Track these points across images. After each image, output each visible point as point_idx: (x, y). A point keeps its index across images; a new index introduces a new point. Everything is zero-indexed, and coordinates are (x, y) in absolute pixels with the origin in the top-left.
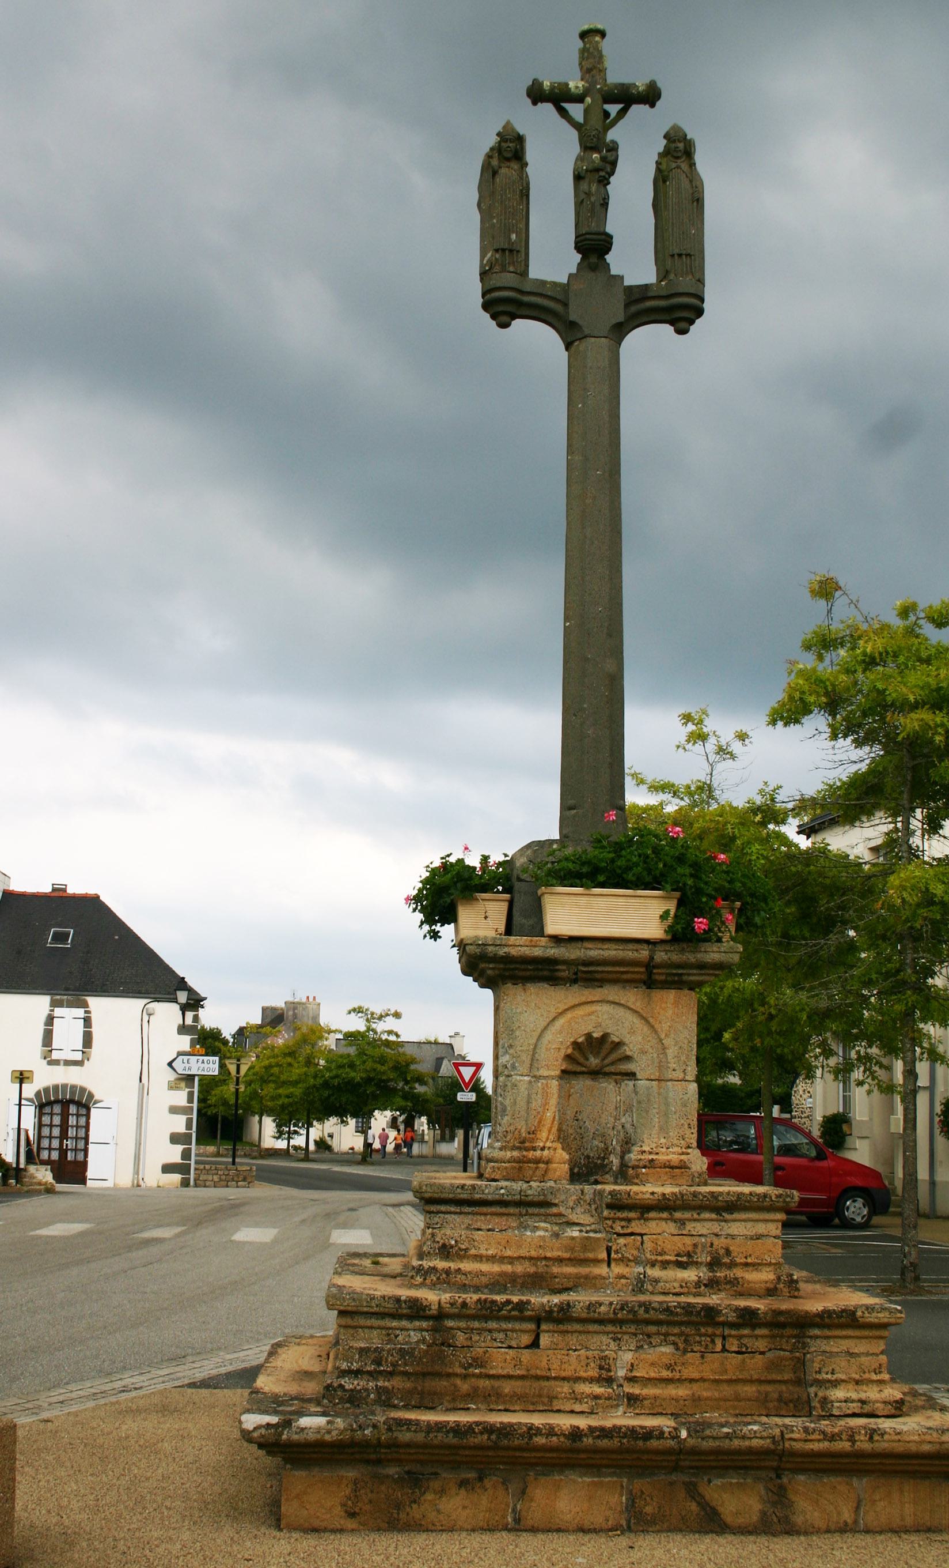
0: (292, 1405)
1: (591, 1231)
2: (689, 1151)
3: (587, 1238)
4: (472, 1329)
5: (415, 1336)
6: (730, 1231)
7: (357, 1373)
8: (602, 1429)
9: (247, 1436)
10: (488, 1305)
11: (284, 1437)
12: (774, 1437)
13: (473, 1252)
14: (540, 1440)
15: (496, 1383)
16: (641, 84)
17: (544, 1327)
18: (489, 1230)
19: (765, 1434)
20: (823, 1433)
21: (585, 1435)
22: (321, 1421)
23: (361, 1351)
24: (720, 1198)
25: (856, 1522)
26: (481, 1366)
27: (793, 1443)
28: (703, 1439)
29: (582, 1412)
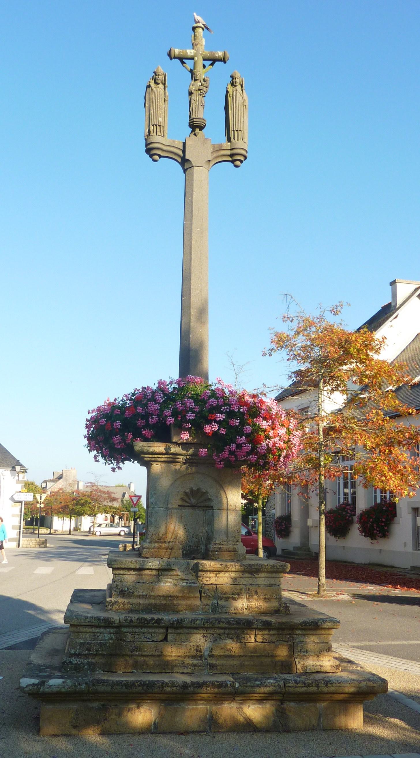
0: (46, 672)
1: (192, 583)
2: (238, 543)
3: (190, 586)
4: (135, 632)
5: (107, 636)
6: (258, 583)
7: (78, 655)
8: (198, 683)
9: (22, 689)
10: (143, 621)
11: (41, 690)
12: (280, 686)
13: (136, 593)
14: (168, 689)
15: (146, 659)
16: (220, 54)
17: (169, 631)
18: (144, 583)
19: (276, 684)
20: (304, 683)
21: (190, 686)
22: (59, 681)
23: (81, 643)
24: (253, 567)
25: (318, 725)
26: (139, 651)
27: (289, 688)
28: (246, 687)
29: (188, 673)
